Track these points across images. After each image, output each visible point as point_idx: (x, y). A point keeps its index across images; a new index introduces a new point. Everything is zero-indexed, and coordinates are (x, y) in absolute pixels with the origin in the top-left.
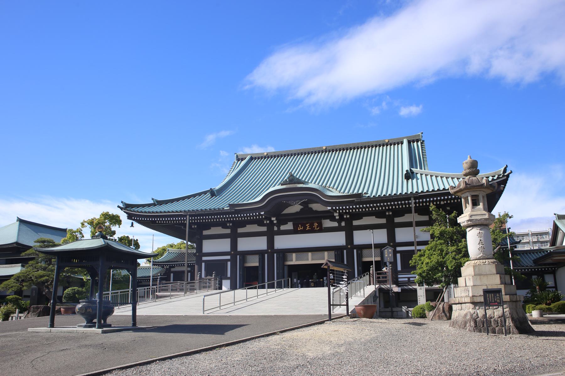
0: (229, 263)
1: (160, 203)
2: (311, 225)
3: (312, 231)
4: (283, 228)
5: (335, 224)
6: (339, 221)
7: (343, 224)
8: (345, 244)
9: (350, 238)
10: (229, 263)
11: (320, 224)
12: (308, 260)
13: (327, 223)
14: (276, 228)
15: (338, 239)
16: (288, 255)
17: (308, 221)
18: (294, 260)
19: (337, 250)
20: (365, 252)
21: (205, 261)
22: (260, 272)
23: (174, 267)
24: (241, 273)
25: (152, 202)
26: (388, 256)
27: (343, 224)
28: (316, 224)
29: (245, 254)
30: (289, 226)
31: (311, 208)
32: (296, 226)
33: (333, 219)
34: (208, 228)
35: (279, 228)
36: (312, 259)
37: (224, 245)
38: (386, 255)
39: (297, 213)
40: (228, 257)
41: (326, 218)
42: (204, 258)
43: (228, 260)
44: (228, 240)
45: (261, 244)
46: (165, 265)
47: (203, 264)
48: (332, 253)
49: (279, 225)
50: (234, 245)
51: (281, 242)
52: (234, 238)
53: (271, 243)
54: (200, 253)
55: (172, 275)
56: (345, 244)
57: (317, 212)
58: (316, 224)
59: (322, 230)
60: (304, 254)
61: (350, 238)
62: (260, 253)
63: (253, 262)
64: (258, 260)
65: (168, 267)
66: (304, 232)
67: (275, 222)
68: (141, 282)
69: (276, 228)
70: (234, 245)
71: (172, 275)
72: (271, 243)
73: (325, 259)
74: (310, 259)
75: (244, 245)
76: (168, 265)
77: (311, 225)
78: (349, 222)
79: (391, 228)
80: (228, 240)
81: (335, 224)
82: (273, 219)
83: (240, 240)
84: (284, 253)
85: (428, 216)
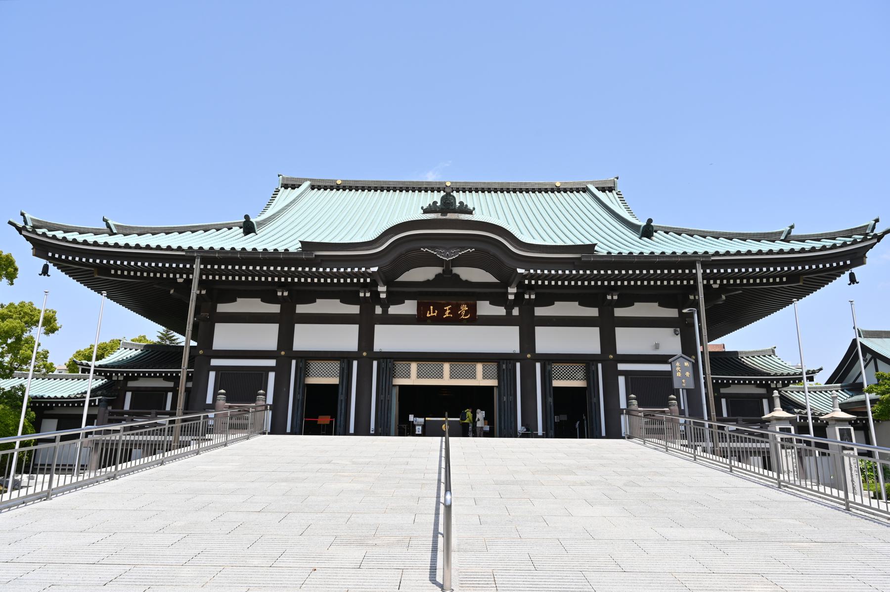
0: (272, 376)
2: (455, 309)
3: (455, 320)
4: (393, 310)
5: (501, 311)
6: (509, 307)
7: (516, 312)
8: (517, 350)
9: (527, 339)
10: (272, 376)
11: (473, 309)
13: (485, 308)
14: (378, 310)
15: (506, 340)
16: (400, 365)
17: (445, 302)
18: (413, 377)
20: (314, 365)
21: (217, 369)
22: (341, 397)
23: (728, 385)
24: (594, 400)
26: (684, 376)
27: (516, 312)
28: (464, 308)
29: (307, 358)
30: (409, 307)
31: (457, 276)
34: (310, 299)
35: (385, 311)
36: (451, 377)
37: (266, 337)
38: (679, 374)
39: (427, 283)
40: (272, 363)
41: (483, 297)
42: (215, 362)
43: (271, 369)
44: (274, 328)
45: (346, 338)
46: (117, 373)
48: (493, 367)
49: (385, 305)
50: (286, 337)
51: (387, 338)
53: (366, 338)
54: (205, 351)
55: (129, 395)
56: (517, 350)
57: (468, 283)
58: (464, 308)
59: (475, 320)
61: (527, 339)
62: (343, 358)
63: (324, 376)
64: (581, 374)
65: (121, 378)
66: (439, 320)
67: (383, 296)
68: (51, 408)
69: (378, 310)
70: (286, 337)
71: (129, 395)
72: (366, 338)
73: (481, 377)
74: (447, 377)
75: (306, 338)
76: (122, 373)
77: (455, 309)
78: (528, 308)
79: (608, 327)
80: (274, 328)
81: (501, 311)
82: (382, 289)
83: (298, 328)
84: (392, 360)
85: (676, 310)
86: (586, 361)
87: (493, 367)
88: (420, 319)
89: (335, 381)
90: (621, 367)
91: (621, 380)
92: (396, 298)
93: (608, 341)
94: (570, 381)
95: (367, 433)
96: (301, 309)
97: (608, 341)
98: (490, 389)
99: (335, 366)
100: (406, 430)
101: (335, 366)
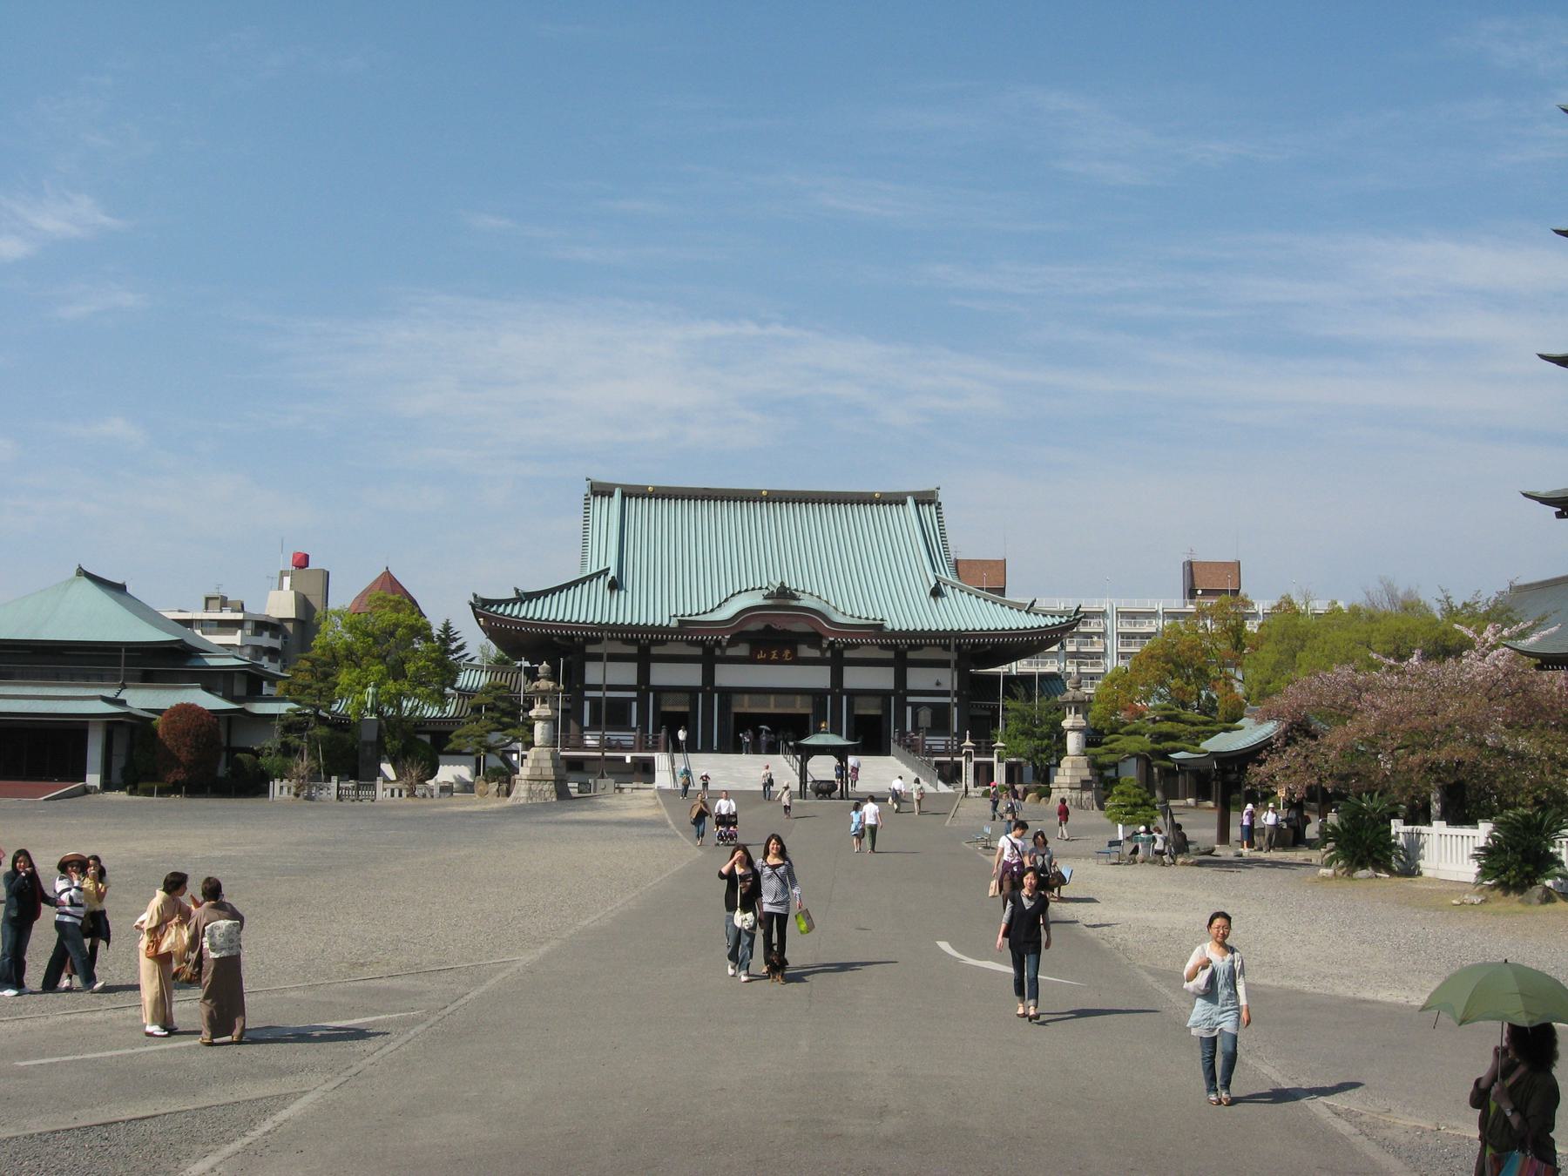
0: (634, 705)
5: (816, 653)
6: (823, 651)
9: (837, 677)
10: (634, 705)
11: (794, 651)
12: (768, 705)
13: (805, 651)
14: (718, 652)
15: (819, 678)
18: (744, 706)
19: (817, 695)
21: (590, 699)
25: (513, 595)
27: (828, 654)
28: (787, 652)
29: (661, 691)
30: (742, 650)
39: (759, 631)
40: (634, 694)
42: (588, 694)
47: (587, 704)
50: (644, 674)
51: (727, 676)
52: (644, 660)
53: (709, 675)
58: (787, 652)
59: (798, 661)
60: (790, 698)
61: (837, 677)
62: (691, 691)
66: (767, 661)
70: (644, 674)
72: (709, 675)
73: (801, 707)
75: (662, 675)
77: (780, 654)
81: (816, 653)
84: (728, 693)
87: (809, 699)
89: (687, 709)
90: (910, 699)
91: (909, 709)
92: (731, 643)
93: (901, 679)
94: (870, 709)
95: (711, 751)
96: (655, 650)
97: (901, 679)
98: (807, 716)
99: (687, 697)
100: (737, 748)
101: (687, 697)
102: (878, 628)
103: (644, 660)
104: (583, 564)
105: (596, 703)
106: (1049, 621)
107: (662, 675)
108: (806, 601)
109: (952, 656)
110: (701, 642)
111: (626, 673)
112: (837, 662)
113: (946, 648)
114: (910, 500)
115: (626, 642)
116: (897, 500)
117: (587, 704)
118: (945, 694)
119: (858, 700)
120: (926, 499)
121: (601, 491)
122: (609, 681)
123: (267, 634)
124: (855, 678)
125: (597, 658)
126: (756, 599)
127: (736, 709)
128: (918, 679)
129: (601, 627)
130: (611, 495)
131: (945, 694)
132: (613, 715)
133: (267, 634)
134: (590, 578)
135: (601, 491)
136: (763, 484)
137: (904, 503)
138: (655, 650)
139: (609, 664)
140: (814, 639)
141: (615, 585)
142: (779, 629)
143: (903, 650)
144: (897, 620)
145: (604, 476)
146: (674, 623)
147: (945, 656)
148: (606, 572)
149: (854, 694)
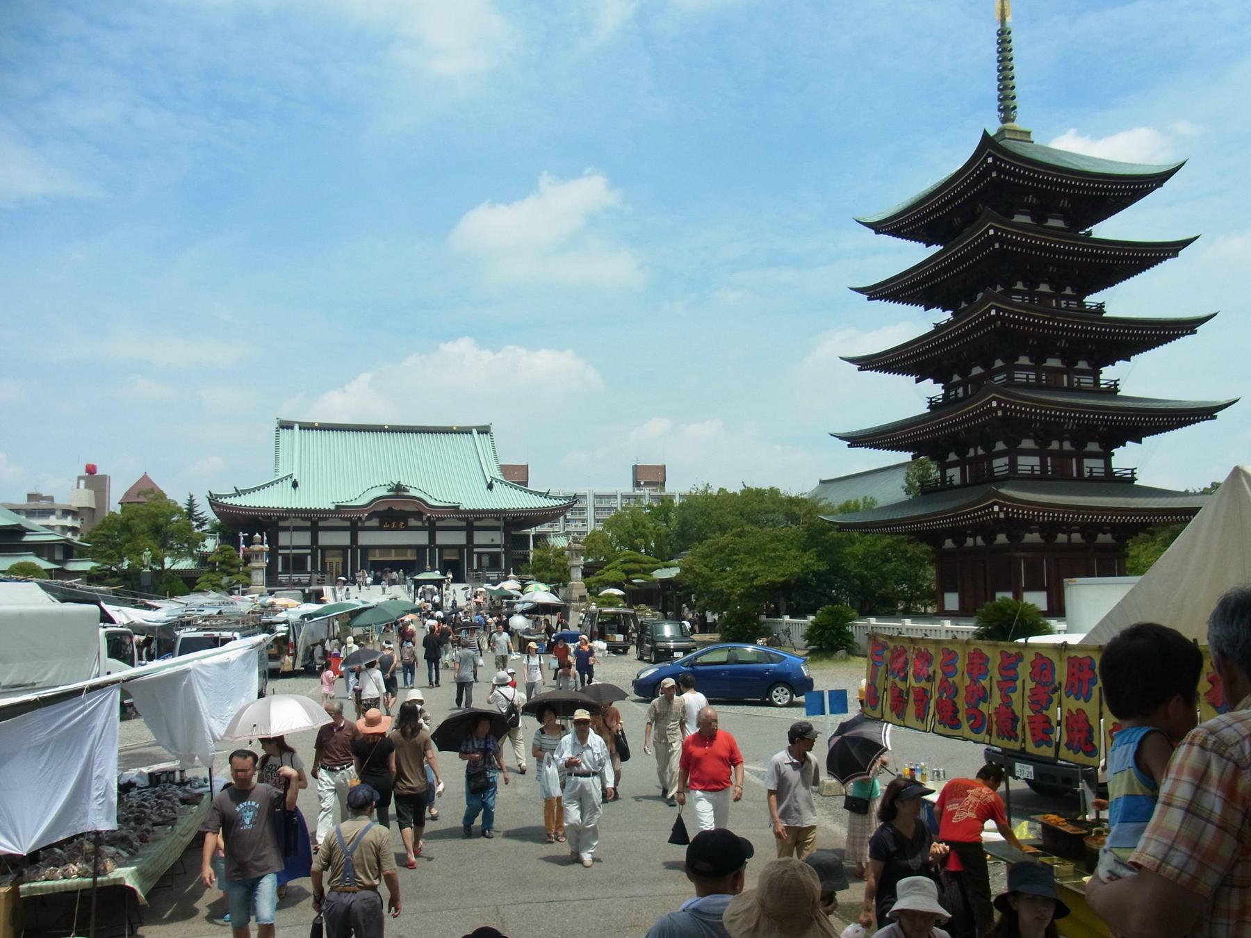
1: (245, 492)
3: (398, 529)
5: (419, 524)
6: (424, 522)
9: (432, 538)
11: (406, 523)
15: (421, 538)
18: (377, 557)
19: (420, 549)
30: (375, 522)
32: (382, 523)
33: (421, 519)
43: (306, 555)
47: (280, 558)
50: (315, 539)
51: (365, 539)
52: (315, 529)
53: (354, 539)
59: (408, 528)
61: (432, 538)
66: (390, 529)
70: (315, 539)
72: (354, 539)
73: (410, 556)
75: (325, 539)
77: (397, 525)
81: (419, 524)
84: (366, 549)
86: (459, 548)
87: (415, 551)
88: (380, 528)
92: (369, 518)
93: (470, 538)
94: (451, 556)
97: (470, 538)
102: (456, 509)
103: (315, 529)
104: (276, 470)
105: (286, 557)
106: (558, 503)
107: (325, 539)
108: (413, 493)
109: (501, 524)
110: (348, 519)
111: (304, 539)
112: (432, 529)
113: (498, 519)
114: (475, 431)
115: (303, 519)
116: (466, 431)
117: (280, 558)
118: (497, 546)
119: (445, 552)
120: (484, 431)
121: (286, 426)
122: (295, 543)
123: (70, 518)
124: (443, 538)
125: (286, 529)
126: (384, 492)
127: (371, 559)
128: (480, 538)
129: (288, 511)
130: (292, 428)
131: (497, 546)
132: (296, 564)
133: (70, 518)
134: (281, 480)
135: (286, 426)
136: (386, 422)
137: (471, 433)
138: (321, 524)
139: (295, 533)
140: (418, 515)
141: (295, 485)
142: (396, 510)
143: (471, 521)
144: (467, 505)
145: (287, 417)
146: (332, 507)
147: (496, 524)
148: (291, 476)
149: (442, 548)
